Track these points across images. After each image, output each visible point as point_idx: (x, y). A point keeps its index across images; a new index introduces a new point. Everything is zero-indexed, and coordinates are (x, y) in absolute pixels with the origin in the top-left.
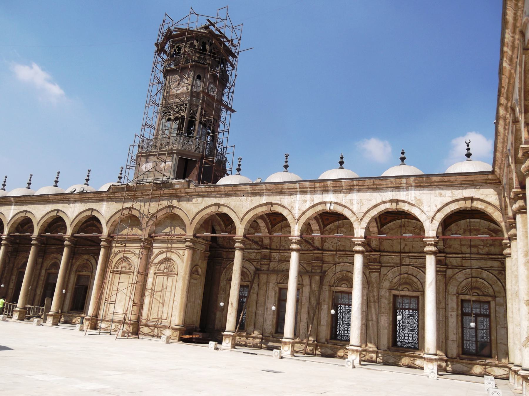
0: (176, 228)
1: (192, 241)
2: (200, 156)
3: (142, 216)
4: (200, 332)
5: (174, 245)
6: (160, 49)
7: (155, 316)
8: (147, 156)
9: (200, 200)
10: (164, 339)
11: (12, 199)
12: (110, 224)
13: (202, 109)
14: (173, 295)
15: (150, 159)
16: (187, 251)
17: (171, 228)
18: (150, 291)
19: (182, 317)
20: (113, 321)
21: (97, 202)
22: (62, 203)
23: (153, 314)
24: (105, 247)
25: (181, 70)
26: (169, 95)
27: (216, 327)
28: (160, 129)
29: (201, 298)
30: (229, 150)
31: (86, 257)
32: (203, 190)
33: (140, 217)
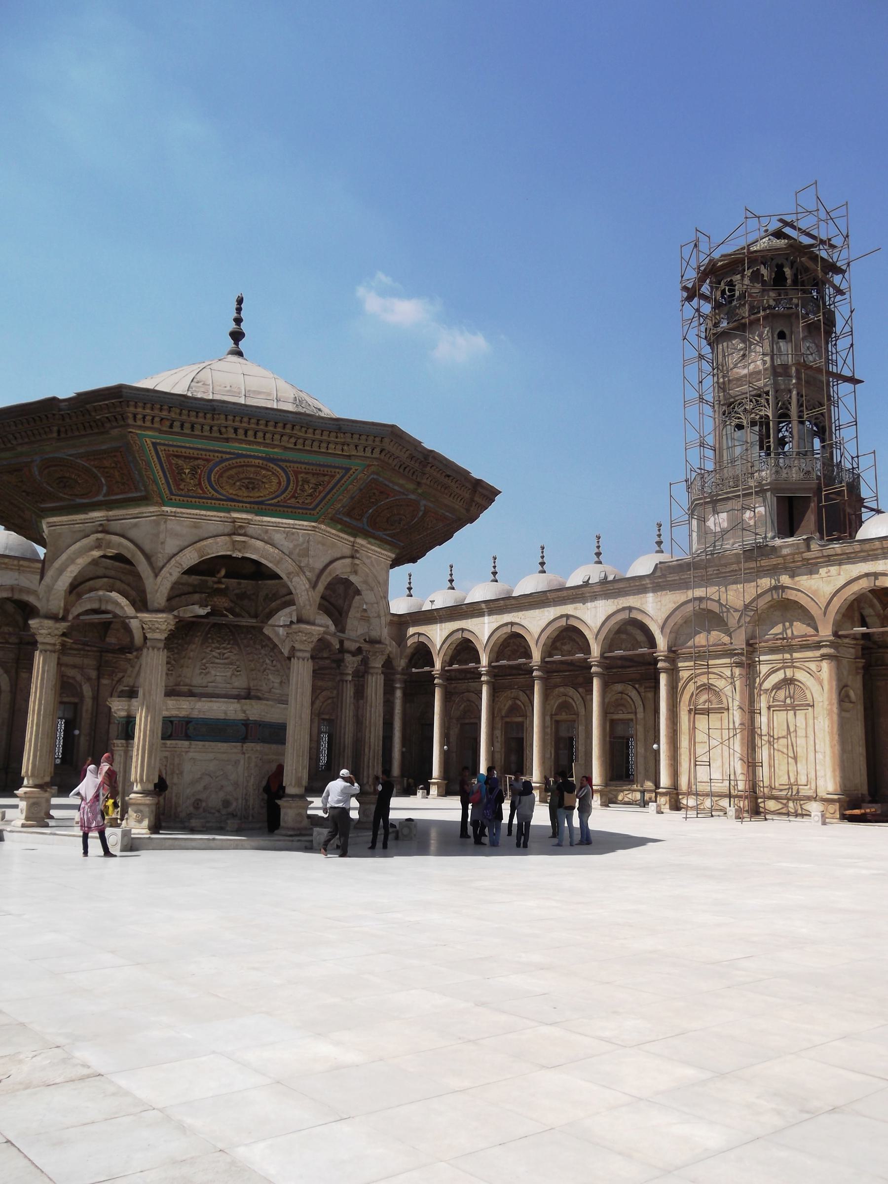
0: (795, 623)
1: (832, 645)
2: (814, 486)
3: (725, 609)
4: (871, 802)
5: (795, 655)
6: (691, 294)
7: (784, 780)
8: (714, 503)
9: (834, 569)
10: (816, 818)
11: (483, 606)
12: (667, 630)
13: (799, 395)
14: (812, 743)
15: (719, 507)
16: (825, 665)
17: (784, 625)
18: (765, 738)
19: (838, 779)
20: (710, 794)
21: (634, 594)
22: (572, 603)
23: (779, 777)
24: (666, 670)
25: (741, 329)
26: (729, 381)
28: (725, 447)
29: (863, 742)
30: (865, 463)
31: (619, 687)
32: (839, 551)
33: (723, 612)
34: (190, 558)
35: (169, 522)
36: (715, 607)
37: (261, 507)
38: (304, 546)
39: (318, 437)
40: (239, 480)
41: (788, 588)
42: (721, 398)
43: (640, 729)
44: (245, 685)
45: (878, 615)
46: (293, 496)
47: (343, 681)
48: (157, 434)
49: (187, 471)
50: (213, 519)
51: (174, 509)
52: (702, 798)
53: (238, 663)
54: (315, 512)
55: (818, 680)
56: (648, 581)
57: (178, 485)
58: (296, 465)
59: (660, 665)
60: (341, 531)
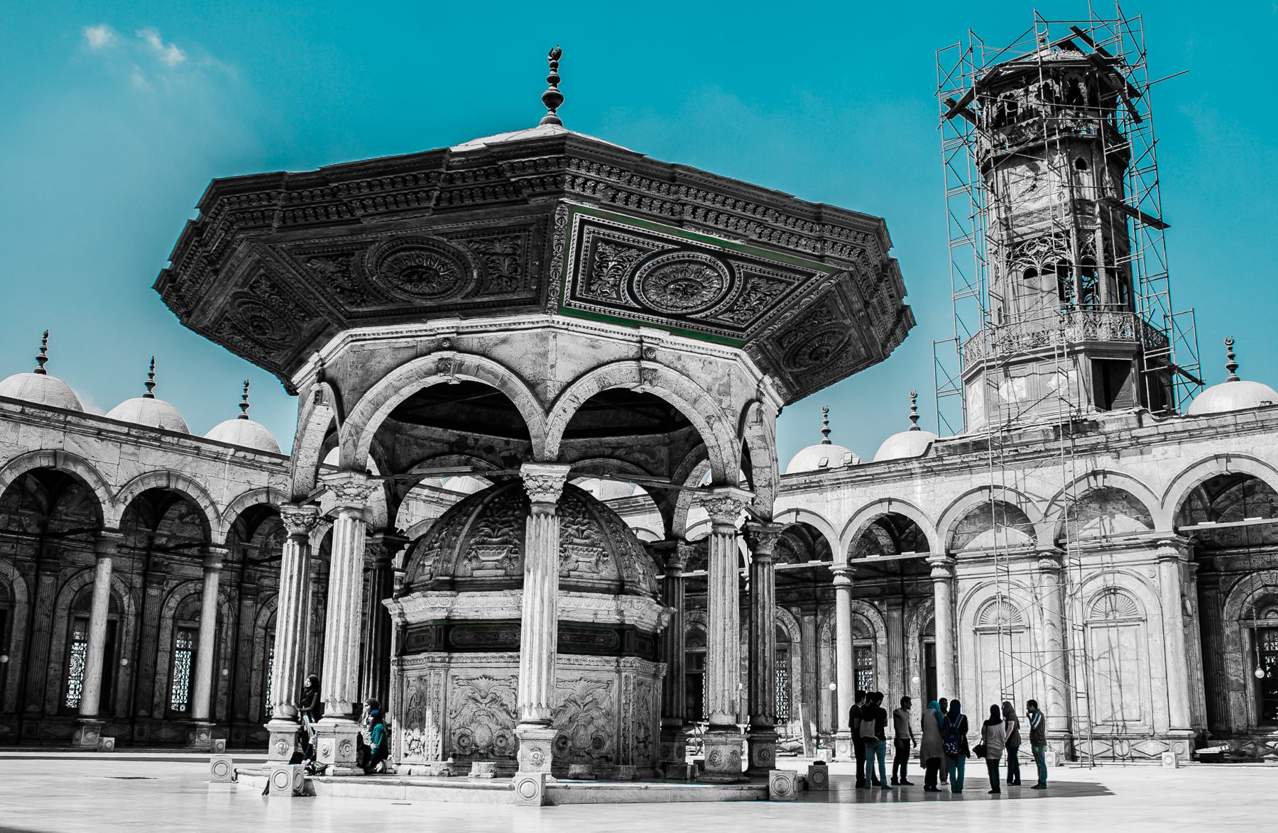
1: (1175, 544)
3: (1023, 499)
7: (1107, 714)
9: (1172, 449)
12: (945, 527)
14: (1145, 667)
15: (1013, 371)
23: (1102, 712)
25: (1030, 155)
27: (1234, 727)
34: (587, 389)
35: (559, 337)
36: (1012, 498)
37: (682, 324)
40: (675, 282)
41: (1111, 473)
42: (1005, 237)
43: (882, 660)
44: (614, 575)
45: (1205, 509)
46: (730, 310)
47: (673, 578)
48: (596, 208)
49: (611, 265)
50: (616, 340)
53: (602, 544)
54: (744, 334)
55: (1158, 588)
57: (589, 283)
58: (750, 266)
60: (757, 363)
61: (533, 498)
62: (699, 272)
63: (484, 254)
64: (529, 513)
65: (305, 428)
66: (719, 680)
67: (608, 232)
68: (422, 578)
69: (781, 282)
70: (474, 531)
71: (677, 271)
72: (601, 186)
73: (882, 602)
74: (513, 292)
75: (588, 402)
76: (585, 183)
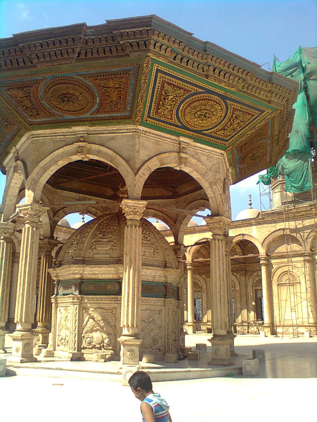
12: (265, 245)
24: (265, 265)
34: (154, 165)
35: (141, 138)
37: (200, 135)
38: (217, 165)
39: (257, 84)
46: (224, 129)
50: (168, 141)
51: (145, 129)
52: (287, 328)
54: (228, 143)
56: (254, 221)
59: (261, 262)
60: (229, 160)
61: (128, 217)
62: (212, 106)
63: (104, 87)
64: (126, 224)
65: (9, 186)
66: (219, 312)
67: (170, 78)
68: (67, 258)
69: (249, 114)
70: (94, 236)
71: (202, 105)
72: (169, 49)
73: (237, 273)
74: (118, 111)
75: (154, 171)
76: (161, 46)
